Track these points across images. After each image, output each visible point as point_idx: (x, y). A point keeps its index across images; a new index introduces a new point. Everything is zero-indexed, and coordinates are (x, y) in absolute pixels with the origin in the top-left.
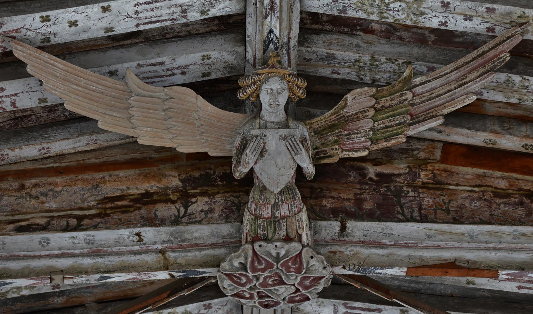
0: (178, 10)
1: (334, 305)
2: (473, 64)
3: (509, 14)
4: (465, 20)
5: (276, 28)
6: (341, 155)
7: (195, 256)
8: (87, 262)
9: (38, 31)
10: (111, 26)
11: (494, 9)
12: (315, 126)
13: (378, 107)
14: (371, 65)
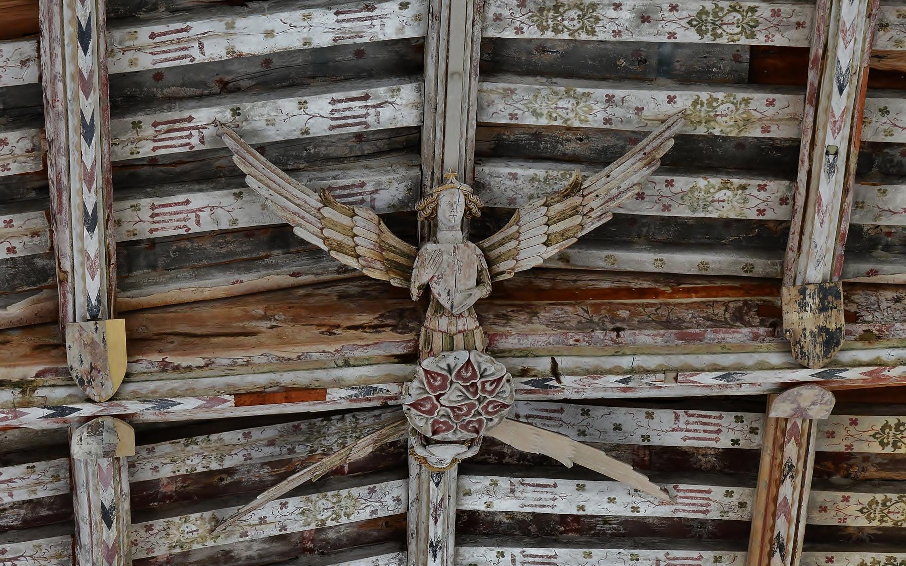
0: (518, 494)
1: (379, 123)
3: (228, 537)
4: (265, 517)
5: (433, 490)
9: (643, 500)
10: (578, 493)
11: (241, 537)
14: (345, 437)
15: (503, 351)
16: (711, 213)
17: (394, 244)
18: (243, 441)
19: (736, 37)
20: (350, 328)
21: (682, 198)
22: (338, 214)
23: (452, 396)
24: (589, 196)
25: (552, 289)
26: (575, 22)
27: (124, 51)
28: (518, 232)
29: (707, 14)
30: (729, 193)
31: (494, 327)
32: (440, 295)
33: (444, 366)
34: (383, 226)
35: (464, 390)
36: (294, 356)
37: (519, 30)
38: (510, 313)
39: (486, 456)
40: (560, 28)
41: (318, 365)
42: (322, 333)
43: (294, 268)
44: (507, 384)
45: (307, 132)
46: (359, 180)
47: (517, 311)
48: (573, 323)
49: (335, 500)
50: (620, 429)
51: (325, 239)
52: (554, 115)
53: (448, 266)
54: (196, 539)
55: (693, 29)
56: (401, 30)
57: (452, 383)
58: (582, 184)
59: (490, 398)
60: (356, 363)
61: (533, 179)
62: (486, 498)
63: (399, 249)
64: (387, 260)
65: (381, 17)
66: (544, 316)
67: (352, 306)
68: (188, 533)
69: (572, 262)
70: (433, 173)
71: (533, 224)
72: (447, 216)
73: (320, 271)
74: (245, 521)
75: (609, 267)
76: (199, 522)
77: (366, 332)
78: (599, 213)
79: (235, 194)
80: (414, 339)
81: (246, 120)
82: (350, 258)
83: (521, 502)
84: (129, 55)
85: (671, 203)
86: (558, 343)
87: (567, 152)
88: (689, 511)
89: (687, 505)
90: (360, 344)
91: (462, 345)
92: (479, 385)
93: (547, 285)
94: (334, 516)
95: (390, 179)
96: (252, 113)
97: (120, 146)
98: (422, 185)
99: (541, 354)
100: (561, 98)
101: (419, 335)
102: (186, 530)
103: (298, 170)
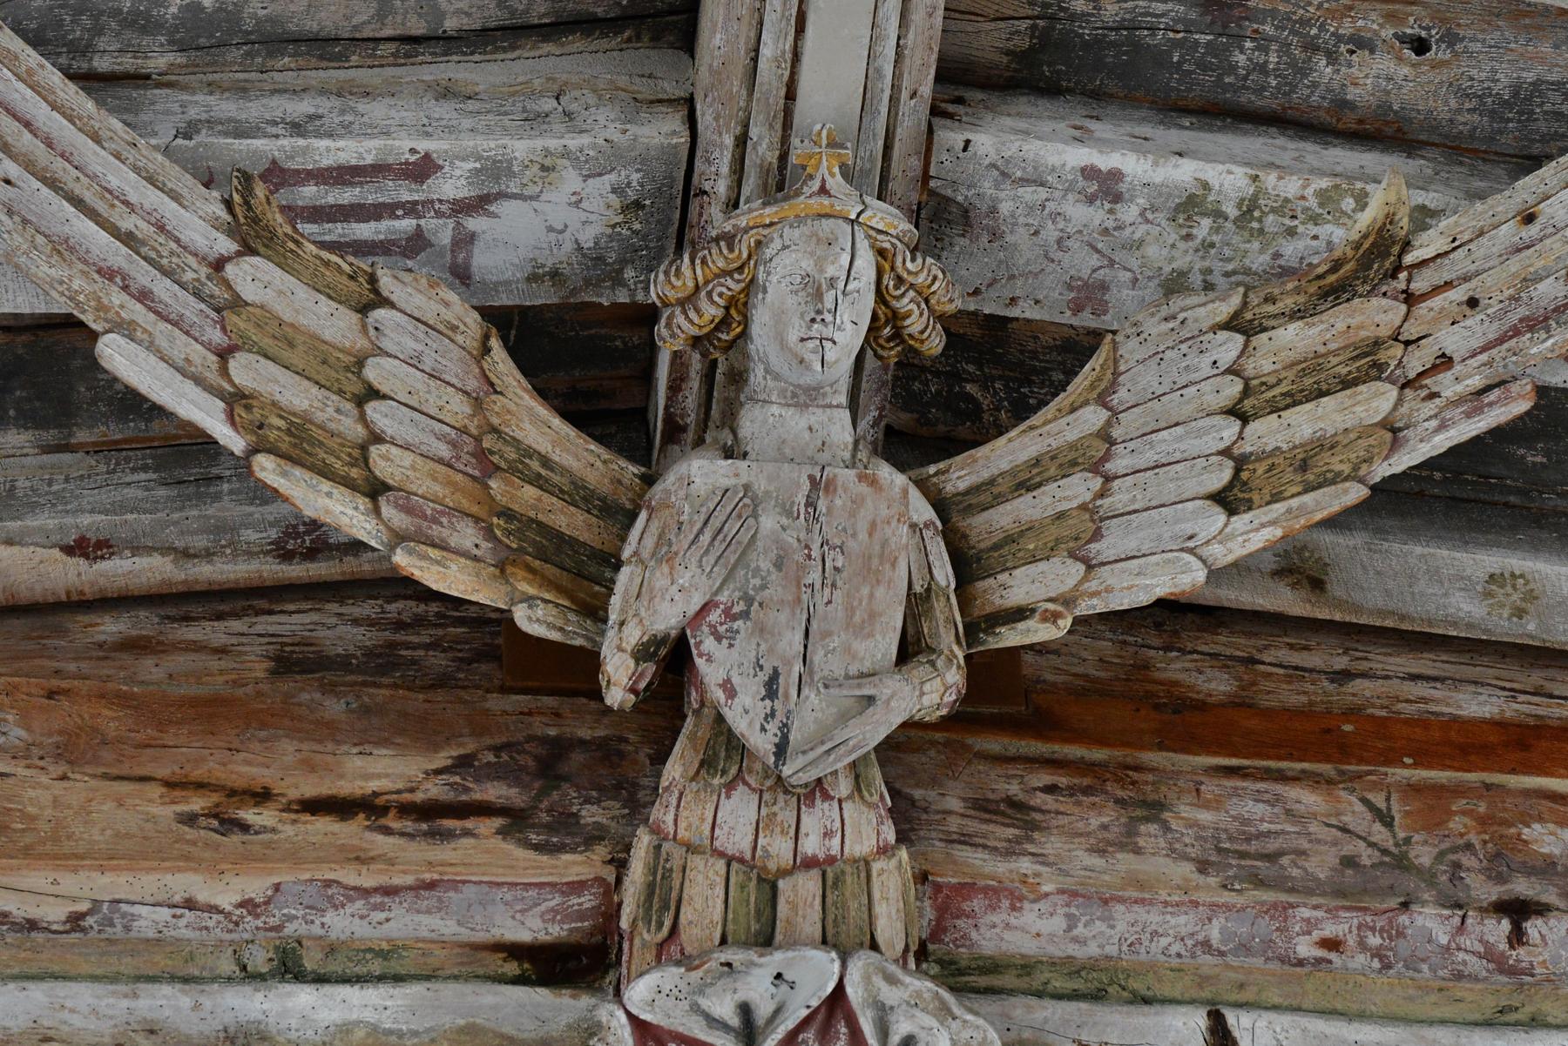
15: (993, 966)
17: (543, 444)
20: (315, 806)
22: (303, 293)
24: (1437, 302)
25: (1239, 704)
28: (1105, 435)
31: (964, 853)
32: (731, 692)
33: (725, 1009)
34: (501, 362)
36: (54, 913)
38: (1040, 799)
41: (162, 962)
42: (190, 819)
43: (86, 520)
46: (404, 147)
47: (1072, 791)
48: (1321, 865)
53: (779, 565)
58: (1406, 245)
60: (334, 967)
61: (1192, 205)
63: (565, 471)
64: (507, 514)
66: (1192, 824)
67: (334, 707)
69: (1336, 589)
70: (742, 141)
71: (1173, 406)
72: (793, 337)
73: (200, 542)
75: (1503, 627)
77: (387, 831)
78: (1476, 382)
80: (599, 880)
82: (339, 492)
86: (1245, 948)
87: (1352, 94)
91: (811, 925)
93: (1217, 685)
95: (547, 152)
98: (690, 191)
99: (1167, 991)
101: (621, 865)
103: (139, 79)
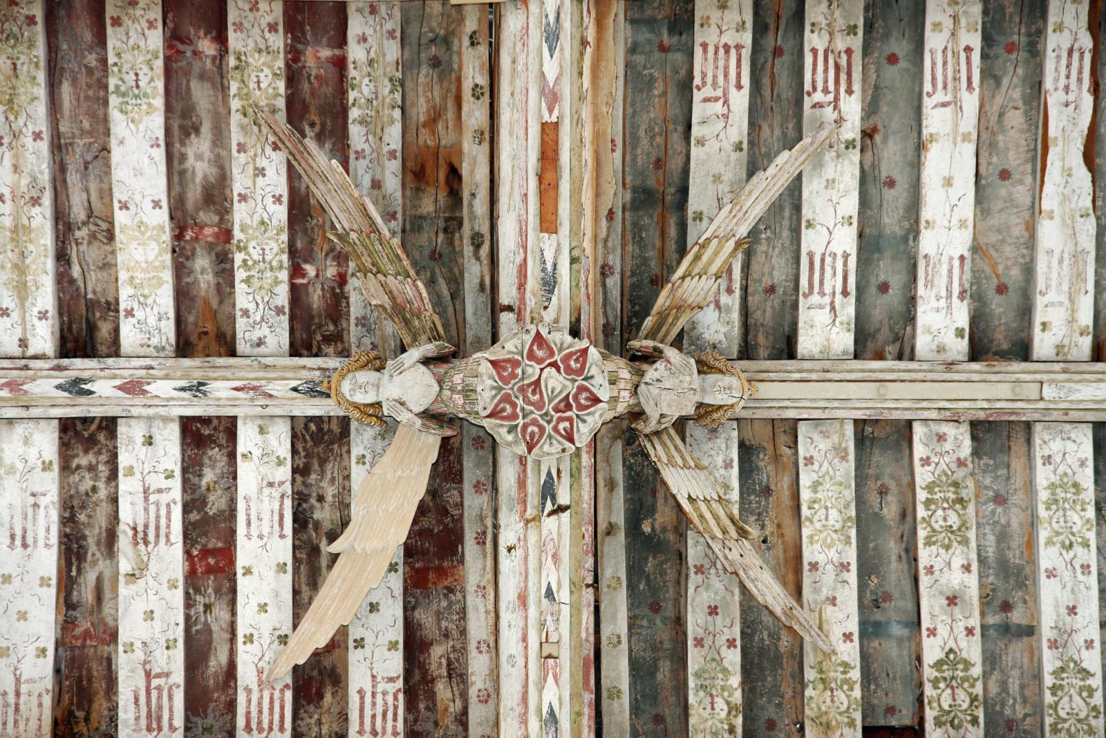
0: (267, 491)
1: (809, 308)
2: (304, 164)
3: (243, 127)
4: (264, 175)
6: (431, 310)
7: (533, 484)
8: (533, 612)
9: (265, 647)
11: (239, 144)
12: (409, 341)
13: (374, 270)
16: (695, 695)
18: (386, 149)
19: (935, 705)
21: (713, 660)
23: (555, 382)
26: (941, 523)
27: (955, 18)
28: (690, 467)
29: (966, 669)
30: (723, 715)
35: (564, 395)
37: (926, 461)
39: (303, 454)
40: (933, 507)
44: (560, 448)
45: (810, 225)
49: (274, 263)
50: (371, 611)
51: (708, 240)
52: (816, 506)
54: (247, 86)
55: (943, 655)
56: (928, 331)
57: (574, 381)
58: (746, 538)
59: (549, 429)
62: (257, 453)
65: (949, 307)
68: (257, 76)
69: (607, 539)
72: (719, 383)
73: (610, 244)
74: (263, 150)
76: (271, 91)
79: (741, 143)
81: (838, 156)
83: (254, 495)
84: (948, 23)
85: (706, 647)
88: (249, 706)
89: (260, 704)
90: (590, 277)
92: (569, 414)
94: (250, 263)
95: (733, 322)
96: (846, 162)
97: (826, 10)
100: (841, 512)
102: (262, 75)
